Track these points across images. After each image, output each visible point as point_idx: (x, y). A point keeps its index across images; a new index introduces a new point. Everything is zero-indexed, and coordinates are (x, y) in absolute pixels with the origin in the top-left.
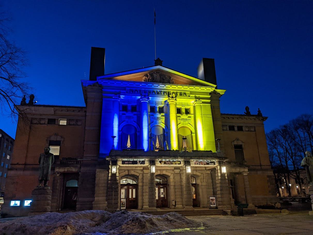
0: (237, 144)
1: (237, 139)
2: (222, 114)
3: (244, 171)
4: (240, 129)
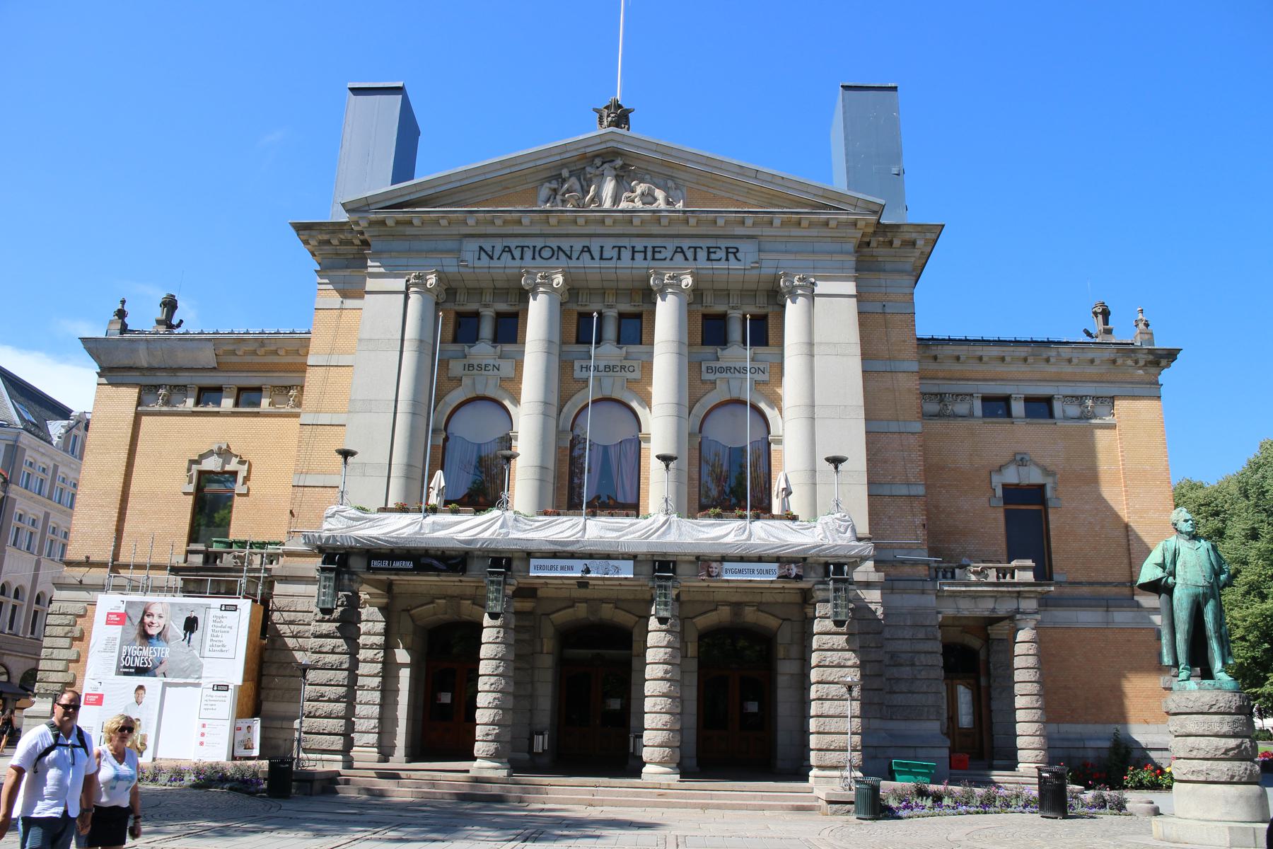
0: (1016, 481)
1: (1018, 457)
2: (924, 343)
3: (1017, 611)
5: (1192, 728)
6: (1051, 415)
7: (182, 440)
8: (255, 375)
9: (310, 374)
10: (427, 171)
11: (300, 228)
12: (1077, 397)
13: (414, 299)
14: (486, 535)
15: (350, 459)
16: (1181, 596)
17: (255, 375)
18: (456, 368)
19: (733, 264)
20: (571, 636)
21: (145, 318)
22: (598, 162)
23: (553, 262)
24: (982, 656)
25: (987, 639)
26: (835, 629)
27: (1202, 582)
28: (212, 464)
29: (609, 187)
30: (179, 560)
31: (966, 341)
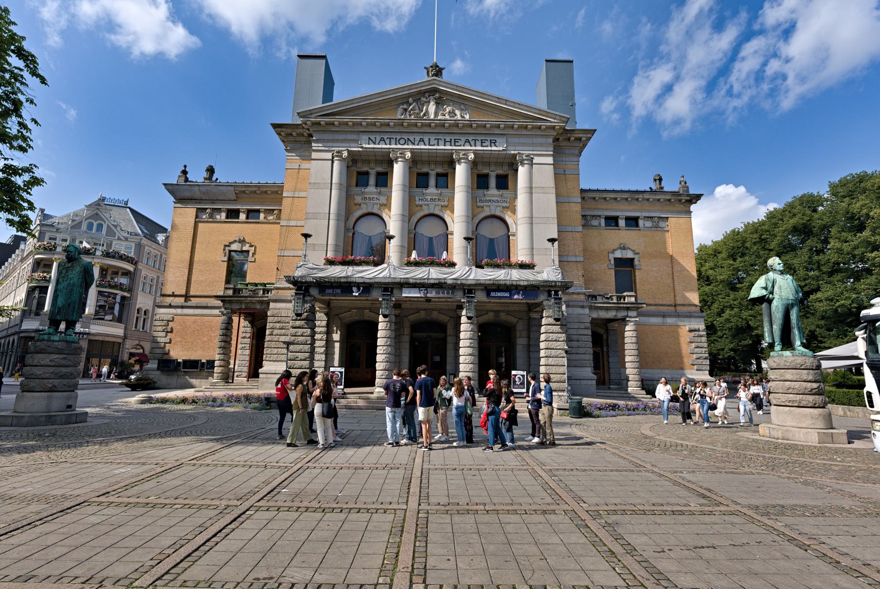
0: (620, 256)
2: (582, 191)
4: (633, 222)
5: (789, 377)
6: (637, 225)
7: (219, 235)
8: (255, 202)
9: (284, 201)
10: (340, 96)
11: (275, 126)
12: (651, 218)
13: (336, 163)
14: (381, 276)
15: (309, 239)
16: (777, 305)
17: (255, 202)
18: (358, 199)
19: (494, 148)
20: (416, 327)
21: (197, 176)
22: (426, 95)
23: (406, 146)
24: (605, 337)
25: (607, 330)
26: (554, 322)
27: (791, 297)
28: (234, 247)
29: (432, 108)
30: (221, 293)
31: (598, 190)
